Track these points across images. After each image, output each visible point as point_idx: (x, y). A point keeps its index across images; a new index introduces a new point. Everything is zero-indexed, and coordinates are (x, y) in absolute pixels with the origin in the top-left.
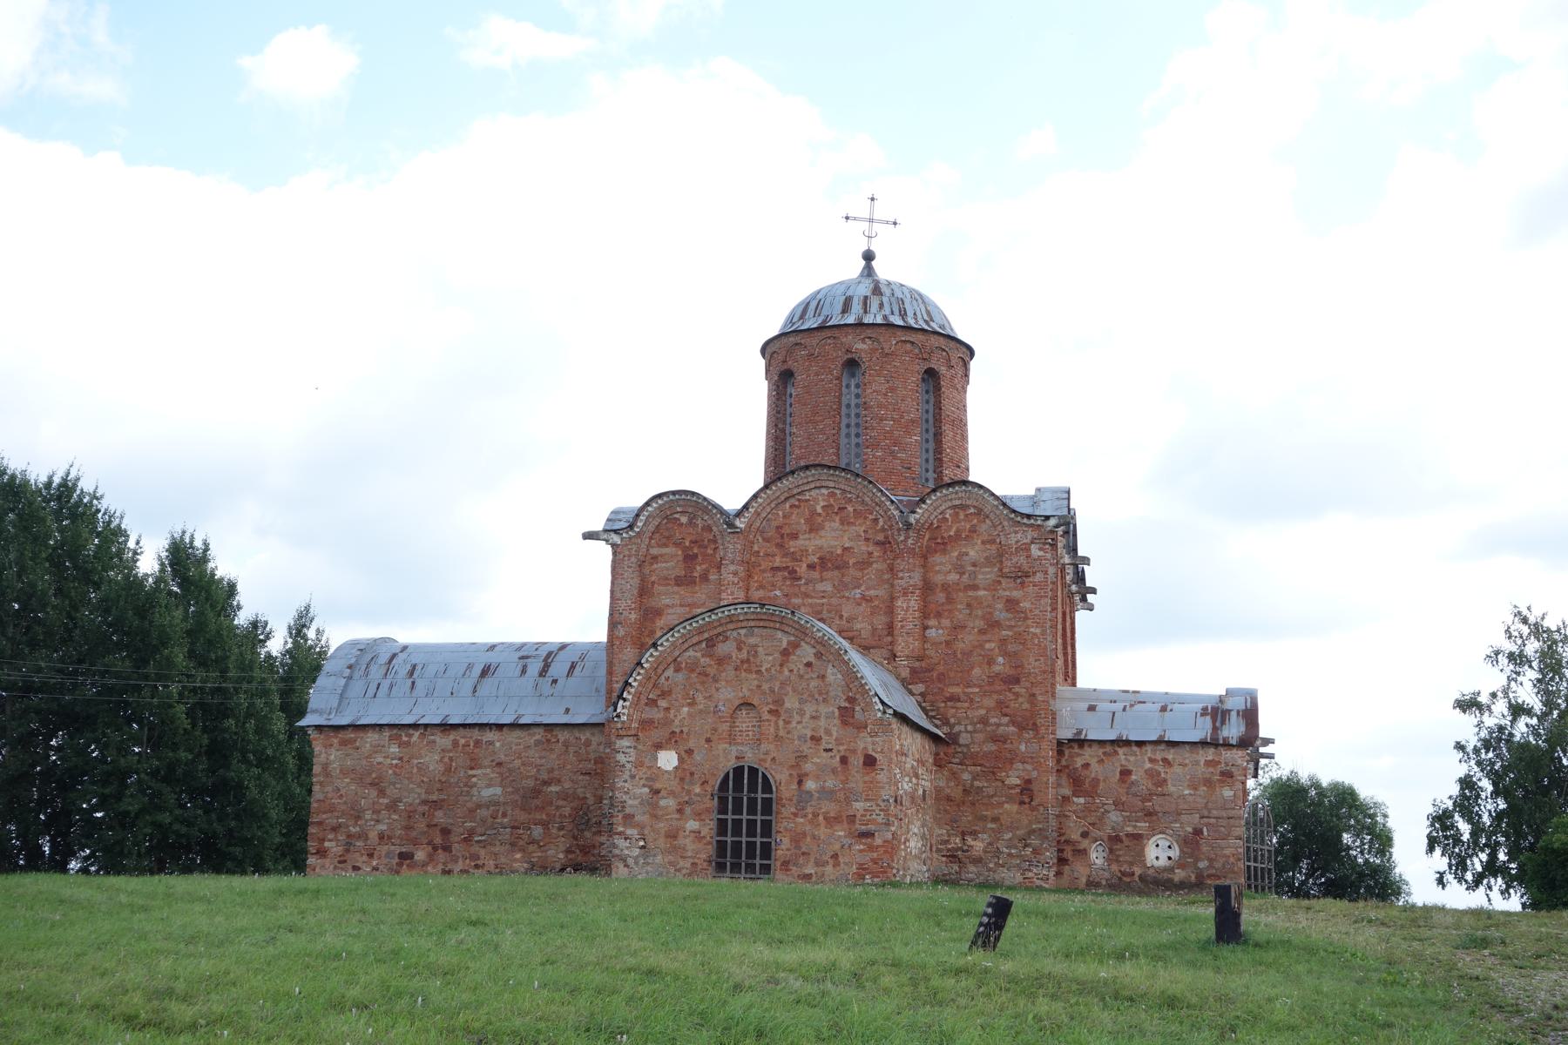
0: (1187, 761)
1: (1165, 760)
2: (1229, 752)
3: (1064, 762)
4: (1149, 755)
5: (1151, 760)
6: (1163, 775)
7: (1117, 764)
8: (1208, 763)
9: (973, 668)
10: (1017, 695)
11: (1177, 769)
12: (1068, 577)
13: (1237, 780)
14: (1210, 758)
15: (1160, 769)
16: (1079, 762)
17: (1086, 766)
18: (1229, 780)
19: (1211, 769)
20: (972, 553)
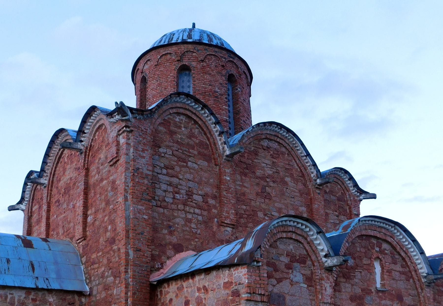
0: (215, 286)
1: (204, 287)
2: (236, 272)
3: (162, 301)
4: (197, 285)
5: (199, 290)
6: (204, 302)
7: (184, 297)
8: (227, 285)
9: (100, 238)
10: (114, 251)
11: (211, 294)
12: (312, 175)
13: (242, 298)
14: (226, 280)
15: (202, 295)
16: (168, 297)
17: (171, 300)
18: (237, 299)
19: (227, 291)
20: (102, 157)
